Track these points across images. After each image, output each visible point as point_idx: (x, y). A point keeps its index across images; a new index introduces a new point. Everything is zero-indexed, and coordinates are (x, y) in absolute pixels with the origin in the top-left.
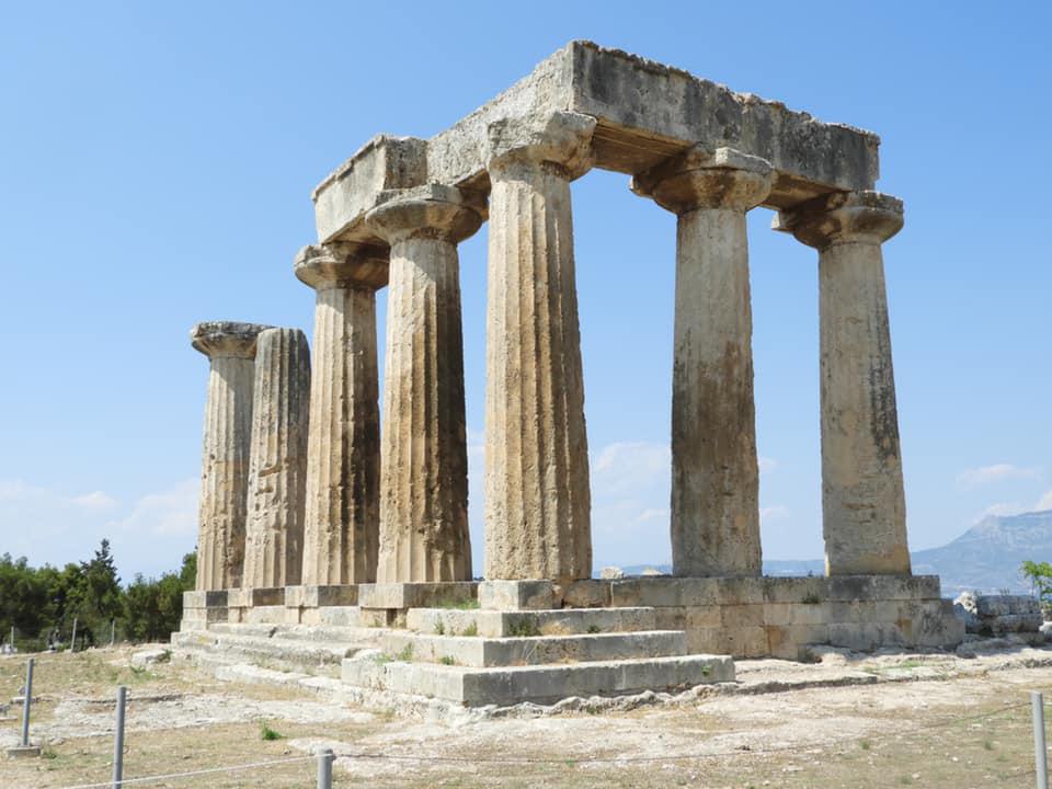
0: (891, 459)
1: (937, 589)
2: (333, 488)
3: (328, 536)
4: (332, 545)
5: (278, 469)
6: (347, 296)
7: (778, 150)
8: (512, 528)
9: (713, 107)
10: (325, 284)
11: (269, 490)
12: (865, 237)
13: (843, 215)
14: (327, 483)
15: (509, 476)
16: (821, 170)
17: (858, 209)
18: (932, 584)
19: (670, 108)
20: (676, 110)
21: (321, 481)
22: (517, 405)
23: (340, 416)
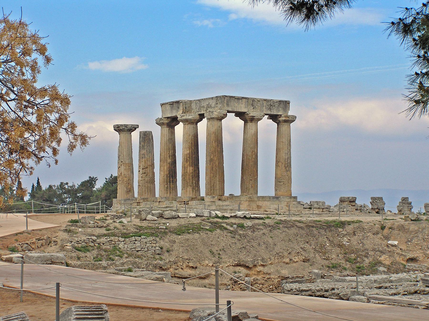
0: (288, 172)
1: (297, 199)
2: (167, 175)
3: (166, 186)
4: (167, 188)
5: (147, 168)
6: (169, 129)
7: (265, 110)
8: (211, 187)
9: (252, 102)
10: (164, 126)
11: (145, 173)
12: (286, 124)
13: (281, 119)
14: (166, 174)
15: (210, 178)
16: (275, 112)
17: (284, 118)
18: (295, 198)
19: (242, 105)
20: (243, 106)
21: (164, 173)
22: (211, 165)
23: (168, 158)
